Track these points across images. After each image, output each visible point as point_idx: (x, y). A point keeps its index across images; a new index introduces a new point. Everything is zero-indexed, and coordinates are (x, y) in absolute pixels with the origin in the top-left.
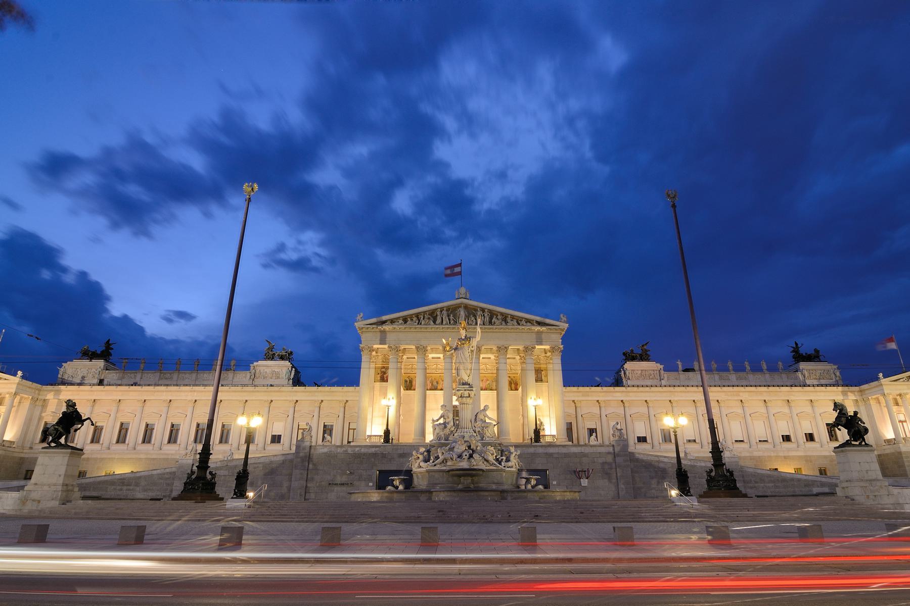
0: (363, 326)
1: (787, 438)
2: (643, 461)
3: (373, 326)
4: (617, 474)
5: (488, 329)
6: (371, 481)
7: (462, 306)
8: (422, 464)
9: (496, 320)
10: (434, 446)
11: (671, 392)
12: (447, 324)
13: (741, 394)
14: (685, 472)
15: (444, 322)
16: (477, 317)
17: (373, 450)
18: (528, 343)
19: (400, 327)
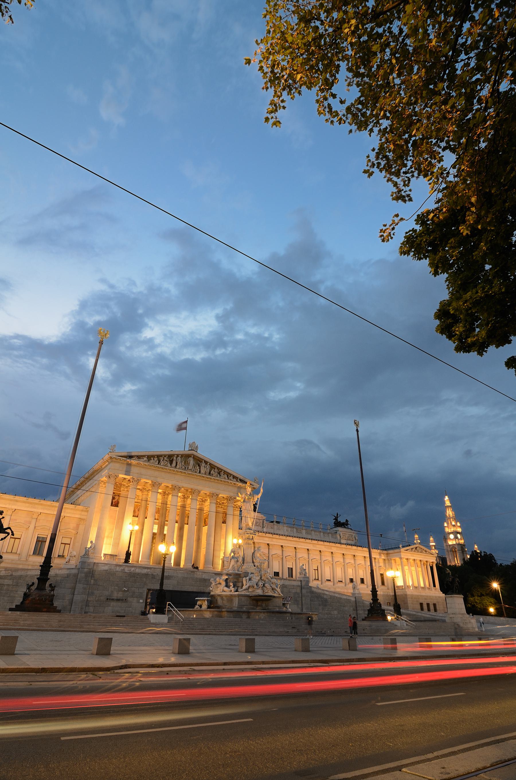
0: (115, 457)
1: (352, 580)
2: (316, 593)
3: (124, 458)
4: (302, 601)
5: (208, 478)
6: (141, 598)
7: (192, 456)
8: (226, 589)
9: (214, 472)
10: (231, 575)
11: (296, 541)
12: (180, 469)
13: (333, 548)
14: (399, 605)
15: (178, 467)
16: (202, 467)
17: (145, 571)
18: (232, 494)
19: (145, 463)
